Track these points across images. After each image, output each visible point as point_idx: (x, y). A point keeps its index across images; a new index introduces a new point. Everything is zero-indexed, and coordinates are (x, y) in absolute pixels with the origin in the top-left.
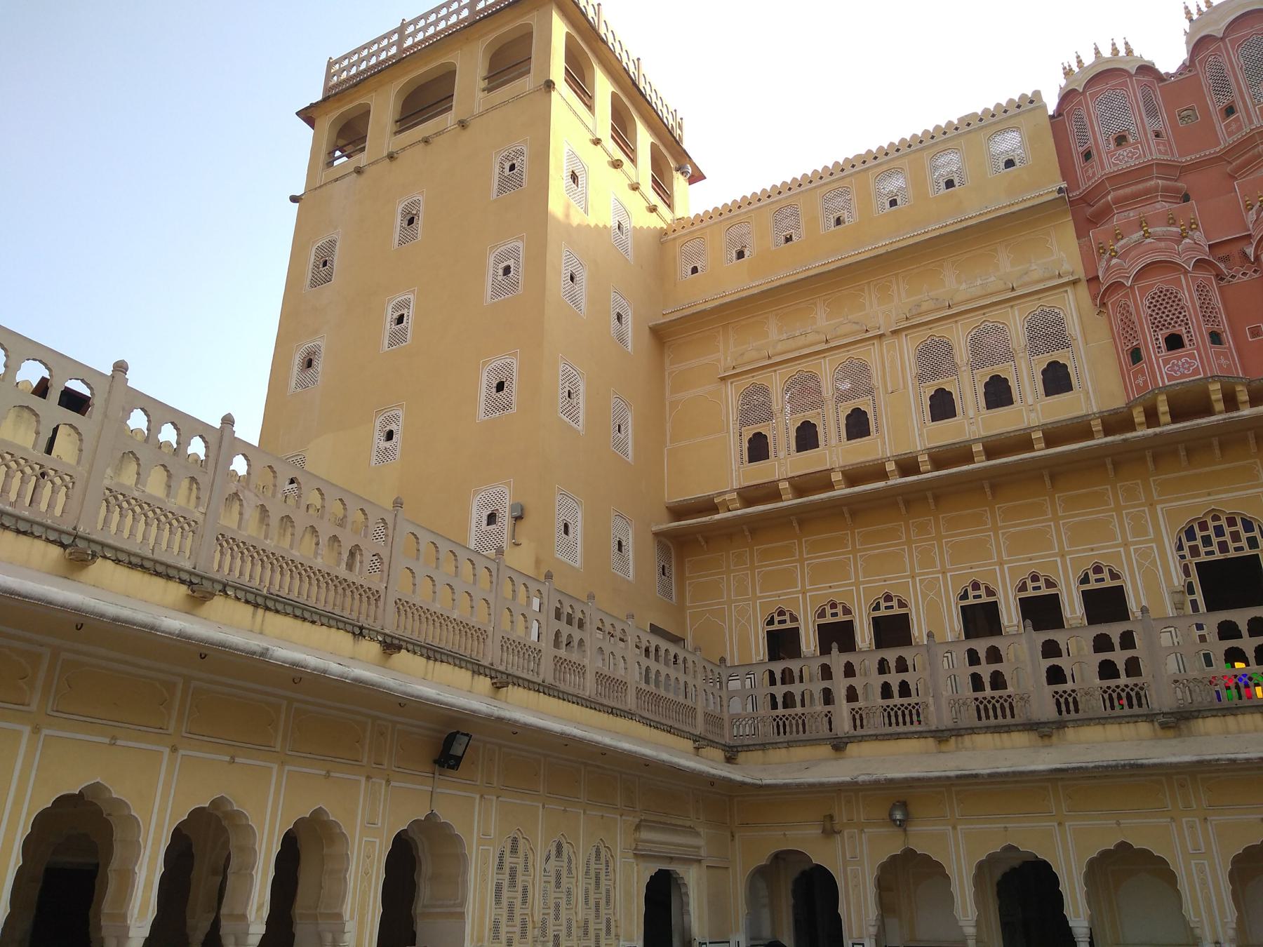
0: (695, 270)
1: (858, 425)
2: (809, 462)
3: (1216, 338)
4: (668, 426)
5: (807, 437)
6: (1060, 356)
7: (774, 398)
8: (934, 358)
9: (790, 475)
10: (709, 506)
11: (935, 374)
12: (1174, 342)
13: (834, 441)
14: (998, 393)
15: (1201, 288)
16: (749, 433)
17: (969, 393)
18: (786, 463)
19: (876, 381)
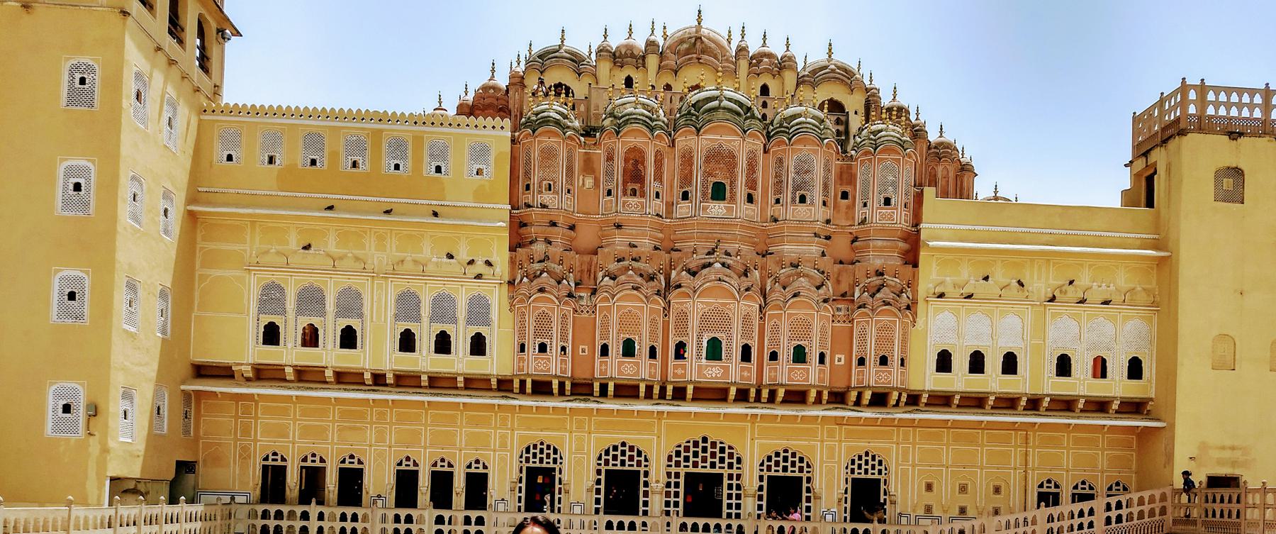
0: (230, 158)
1: (348, 339)
2: (309, 357)
3: (563, 349)
4: (197, 294)
5: (311, 338)
6: (484, 330)
7: (288, 298)
8: (407, 304)
9: (295, 363)
10: (225, 373)
11: (408, 318)
12: (543, 348)
13: (330, 346)
14: (443, 344)
15: (564, 317)
16: (266, 320)
17: (425, 341)
18: (290, 353)
19: (366, 310)
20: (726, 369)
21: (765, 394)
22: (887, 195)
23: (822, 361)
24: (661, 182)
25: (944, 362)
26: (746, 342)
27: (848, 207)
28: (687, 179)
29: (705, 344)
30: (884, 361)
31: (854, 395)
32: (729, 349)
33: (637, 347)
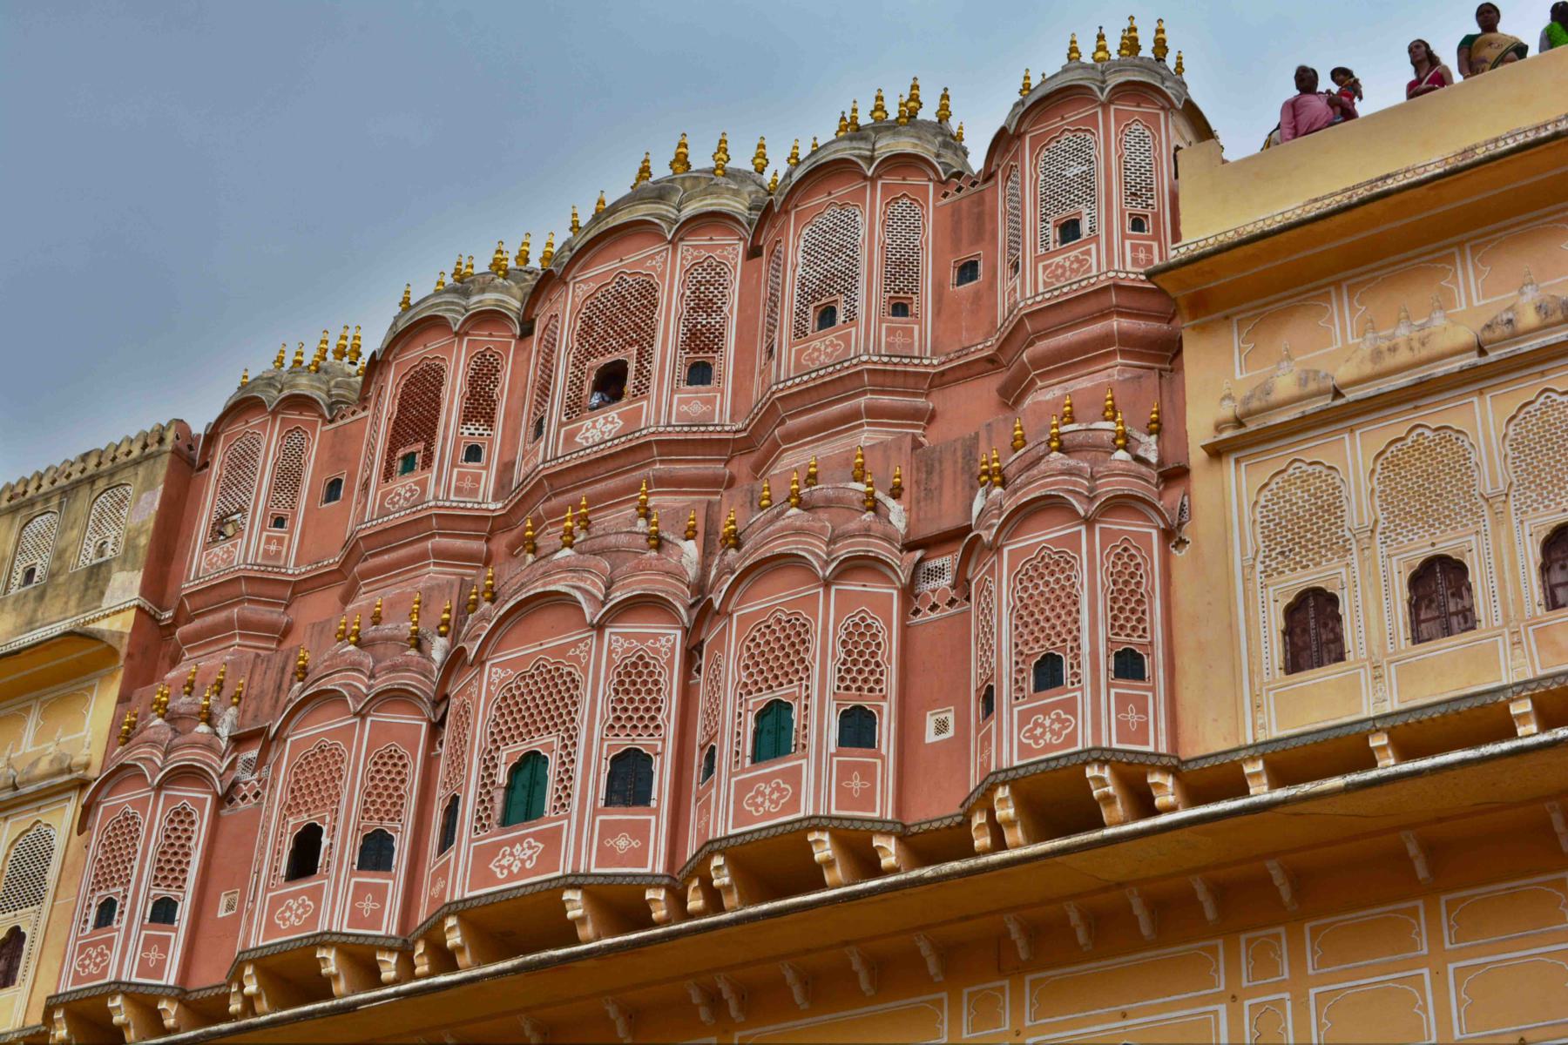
3: (164, 911)
15: (182, 817)
20: (552, 839)
21: (695, 902)
22: (1067, 214)
23: (857, 728)
24: (490, 420)
25: (1313, 629)
26: (624, 742)
27: (977, 297)
28: (544, 390)
29: (502, 777)
30: (1049, 672)
31: (979, 819)
32: (566, 777)
33: (325, 841)
